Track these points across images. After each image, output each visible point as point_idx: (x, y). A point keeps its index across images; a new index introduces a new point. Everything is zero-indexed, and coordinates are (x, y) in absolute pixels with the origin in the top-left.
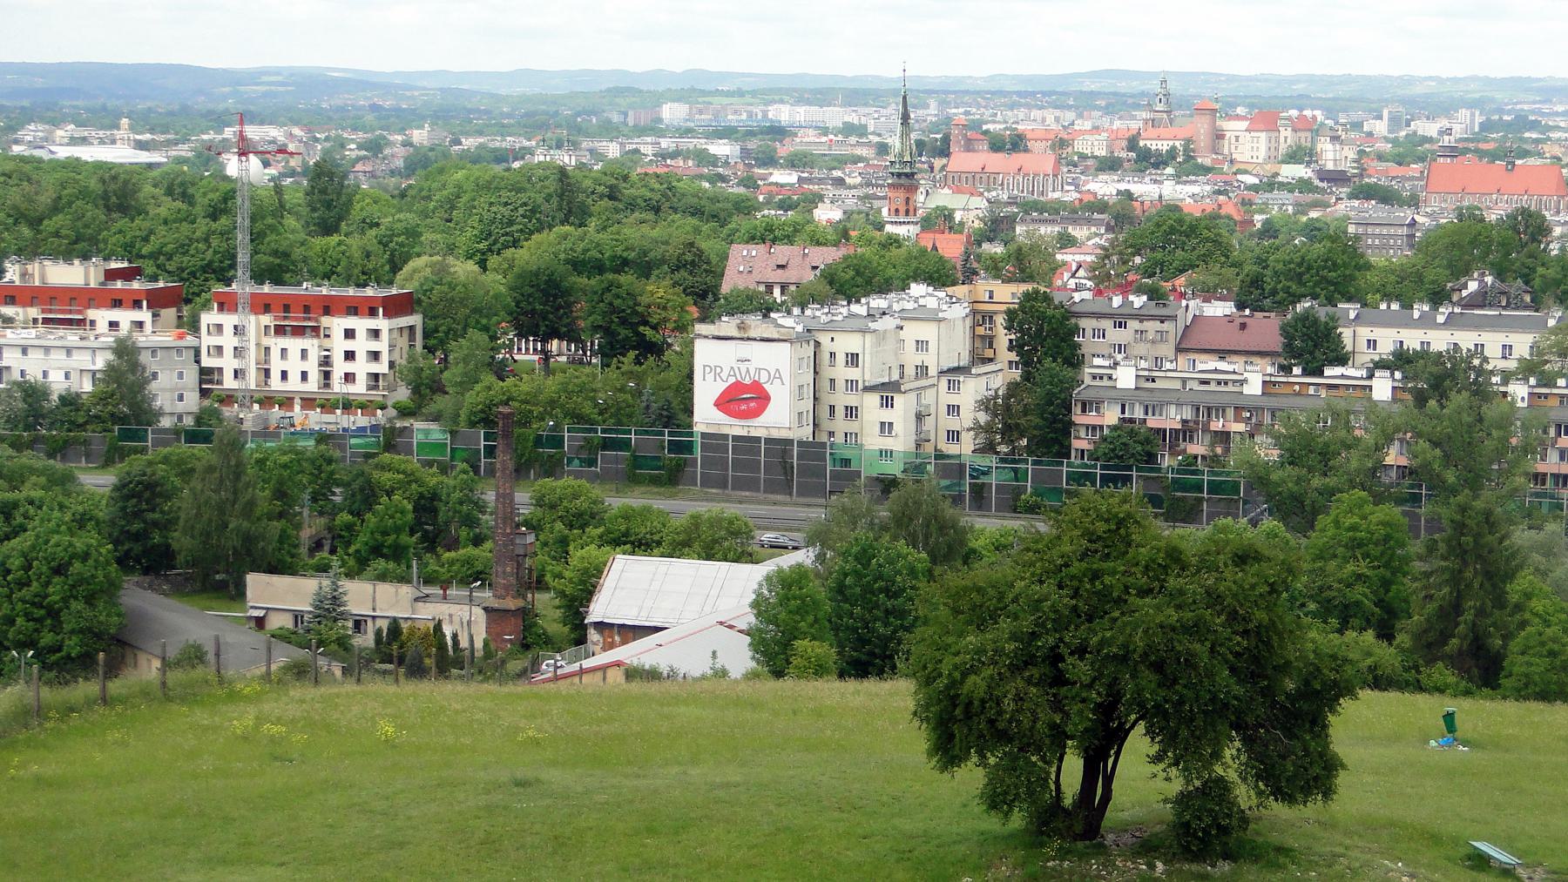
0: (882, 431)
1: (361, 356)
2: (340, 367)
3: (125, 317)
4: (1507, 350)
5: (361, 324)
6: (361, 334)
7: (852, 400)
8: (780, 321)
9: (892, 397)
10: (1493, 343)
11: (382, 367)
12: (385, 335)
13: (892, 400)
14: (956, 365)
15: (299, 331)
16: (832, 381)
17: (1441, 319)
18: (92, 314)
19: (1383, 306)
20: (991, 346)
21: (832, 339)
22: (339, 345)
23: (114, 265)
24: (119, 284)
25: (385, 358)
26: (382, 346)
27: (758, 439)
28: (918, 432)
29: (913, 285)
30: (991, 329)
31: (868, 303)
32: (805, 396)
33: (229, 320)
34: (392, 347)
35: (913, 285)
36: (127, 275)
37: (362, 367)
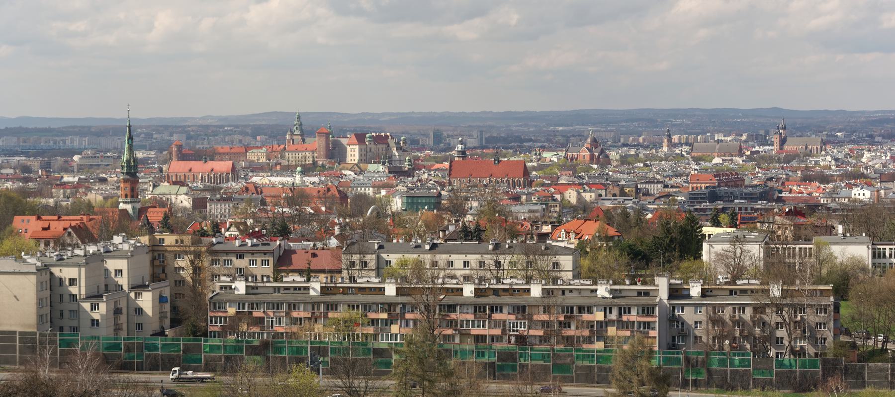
0: (93, 325)
4: (466, 264)
7: (73, 306)
8: (29, 260)
9: (98, 304)
10: (458, 260)
13: (98, 306)
14: (141, 284)
16: (61, 296)
17: (427, 247)
19: (395, 241)
20: (163, 272)
21: (61, 270)
27: (15, 332)
28: (116, 324)
29: (115, 237)
30: (163, 262)
31: (85, 249)
32: (45, 305)
35: (115, 237)
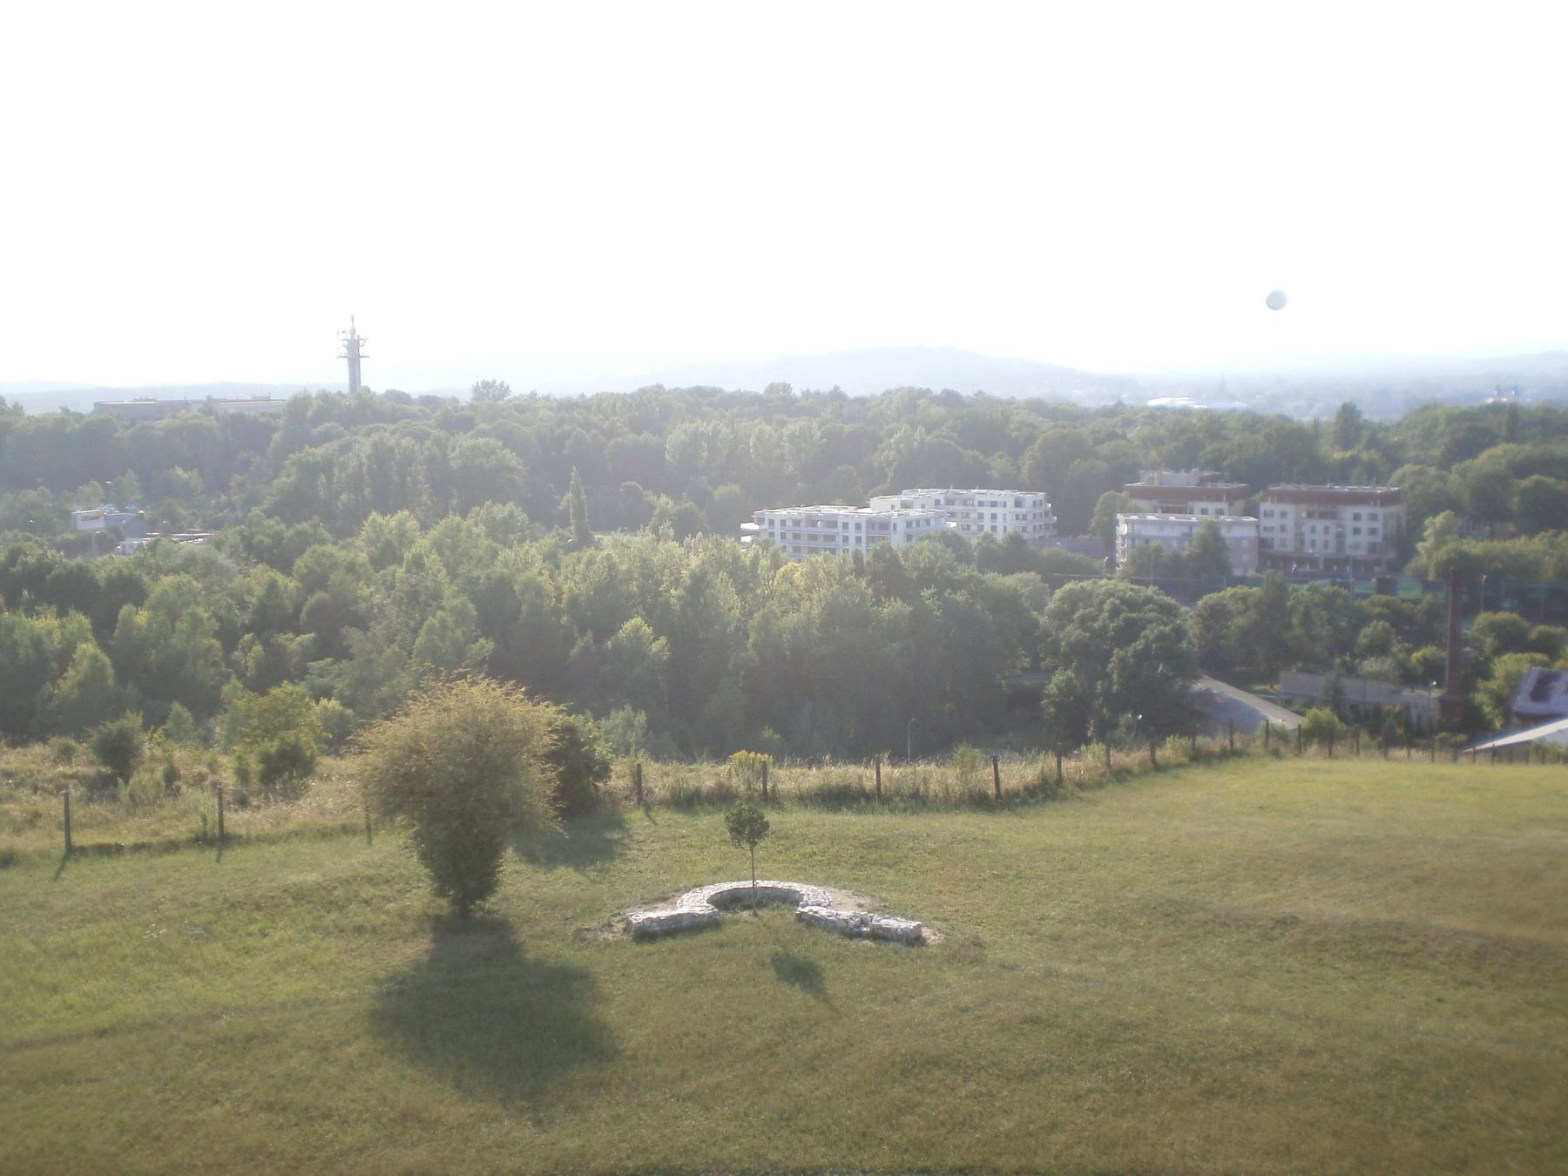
1: (1364, 532)
2: (1350, 539)
3: (1212, 506)
5: (1364, 511)
6: (1364, 517)
11: (1378, 539)
12: (1380, 518)
15: (1323, 516)
18: (1190, 504)
22: (1350, 525)
23: (1206, 474)
24: (1209, 486)
25: (1381, 532)
26: (1379, 525)
33: (1278, 508)
34: (1385, 525)
36: (1214, 479)
37: (1364, 539)
